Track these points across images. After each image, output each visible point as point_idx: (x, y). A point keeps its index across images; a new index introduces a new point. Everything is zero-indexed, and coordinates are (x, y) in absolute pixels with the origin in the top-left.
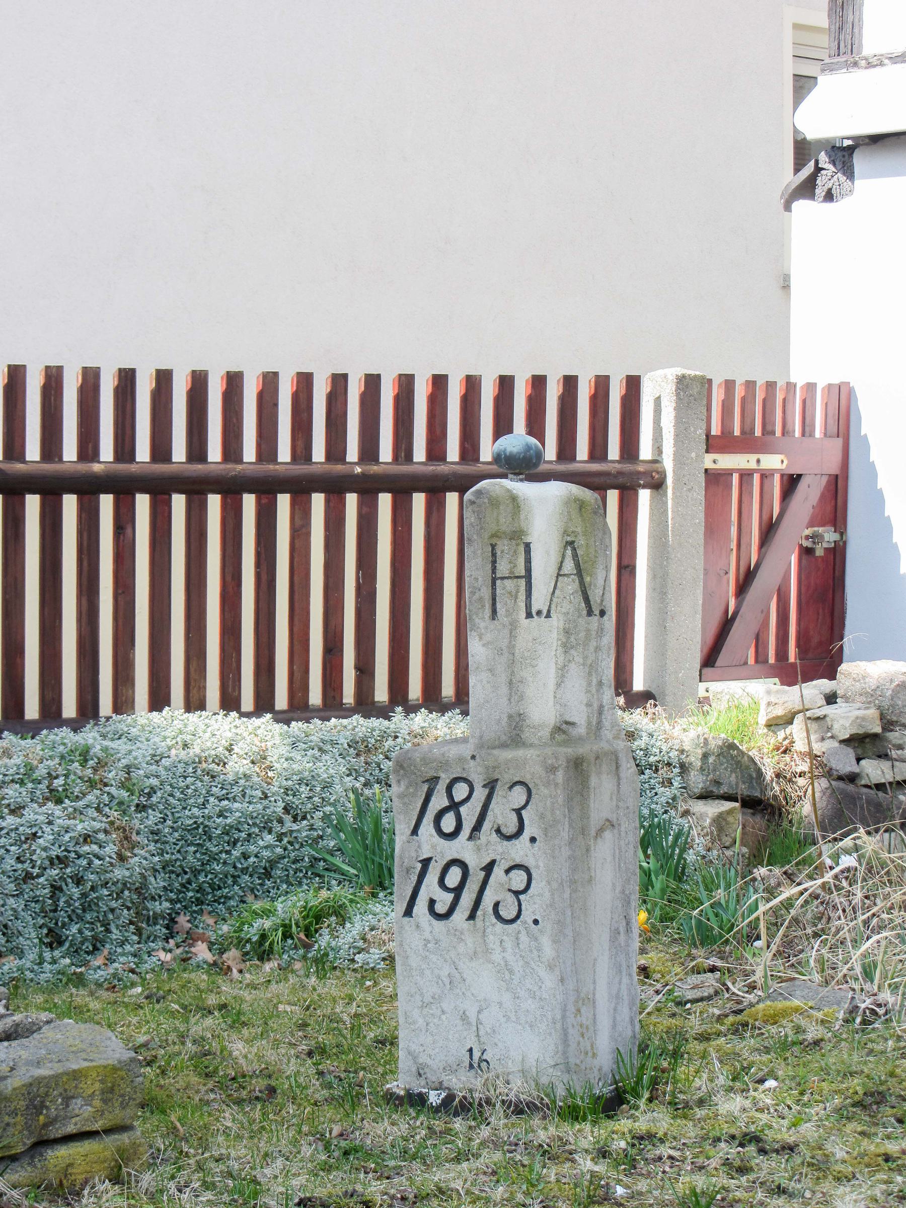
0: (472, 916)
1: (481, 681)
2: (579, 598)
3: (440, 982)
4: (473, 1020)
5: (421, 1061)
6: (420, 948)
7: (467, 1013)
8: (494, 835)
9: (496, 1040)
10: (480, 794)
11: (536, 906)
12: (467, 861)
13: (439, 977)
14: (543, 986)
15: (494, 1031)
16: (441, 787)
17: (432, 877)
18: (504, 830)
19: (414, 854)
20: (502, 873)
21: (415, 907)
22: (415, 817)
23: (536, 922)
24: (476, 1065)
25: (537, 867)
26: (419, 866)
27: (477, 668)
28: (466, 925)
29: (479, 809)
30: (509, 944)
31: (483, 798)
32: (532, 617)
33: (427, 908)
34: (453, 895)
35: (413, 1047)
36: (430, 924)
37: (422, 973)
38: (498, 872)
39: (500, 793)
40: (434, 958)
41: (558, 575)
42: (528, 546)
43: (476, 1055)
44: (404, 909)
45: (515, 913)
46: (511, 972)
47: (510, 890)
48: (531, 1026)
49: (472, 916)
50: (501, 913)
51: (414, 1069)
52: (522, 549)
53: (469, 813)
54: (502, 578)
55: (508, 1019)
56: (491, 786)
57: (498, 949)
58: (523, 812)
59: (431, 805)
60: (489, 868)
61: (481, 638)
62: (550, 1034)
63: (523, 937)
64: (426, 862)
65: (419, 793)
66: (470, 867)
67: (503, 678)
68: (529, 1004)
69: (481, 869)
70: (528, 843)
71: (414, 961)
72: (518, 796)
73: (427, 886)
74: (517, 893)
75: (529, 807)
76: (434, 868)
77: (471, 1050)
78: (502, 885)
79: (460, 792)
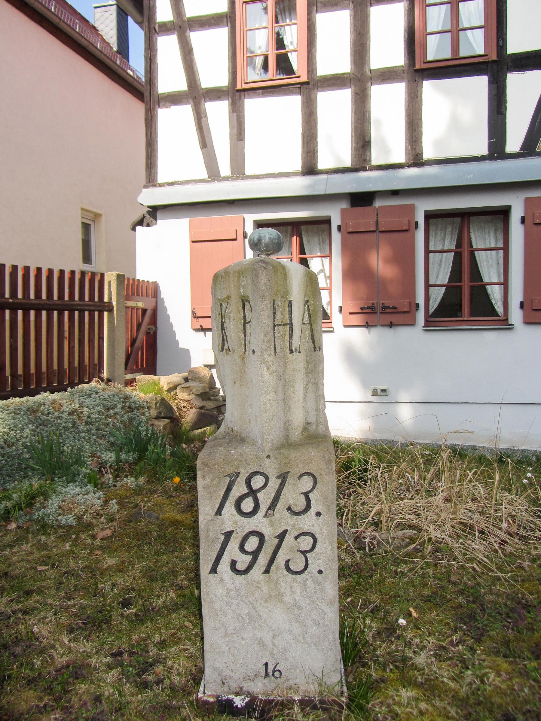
0: (267, 571)
1: (270, 400)
2: (311, 341)
3: (240, 618)
4: (269, 644)
5: (224, 674)
6: (224, 595)
7: (263, 639)
8: (286, 511)
9: (287, 656)
10: (274, 484)
11: (321, 561)
12: (264, 532)
13: (239, 615)
14: (326, 616)
15: (285, 650)
16: (241, 479)
17: (233, 545)
18: (295, 509)
19: (218, 529)
20: (292, 539)
21: (219, 566)
22: (219, 502)
23: (320, 572)
24: (271, 674)
25: (322, 533)
26: (222, 537)
27: (267, 391)
28: (262, 577)
29: (273, 494)
30: (297, 589)
31: (277, 487)
32: (293, 352)
33: (229, 567)
34: (251, 556)
35: (217, 665)
36: (232, 579)
37: (225, 613)
38: (289, 539)
39: (291, 482)
40: (235, 602)
41: (275, 326)
42: (290, 302)
43: (270, 668)
44: (210, 568)
45: (303, 567)
46: (300, 608)
47: (298, 551)
48: (315, 645)
49: (267, 571)
50: (291, 567)
51: (219, 680)
52: (287, 303)
53: (265, 497)
54: (279, 325)
55: (297, 641)
56: (283, 477)
57: (288, 593)
58: (310, 495)
59: (232, 492)
60: (282, 536)
61: (268, 369)
62: (332, 650)
63: (310, 583)
64: (228, 535)
65: (222, 484)
66: (266, 536)
67: (281, 398)
68: (315, 630)
69: (275, 537)
70: (314, 517)
71: (218, 606)
72: (306, 483)
73: (229, 551)
74: (304, 553)
75: (315, 491)
76: (235, 538)
77: (266, 664)
78: (292, 548)
79: (257, 482)
